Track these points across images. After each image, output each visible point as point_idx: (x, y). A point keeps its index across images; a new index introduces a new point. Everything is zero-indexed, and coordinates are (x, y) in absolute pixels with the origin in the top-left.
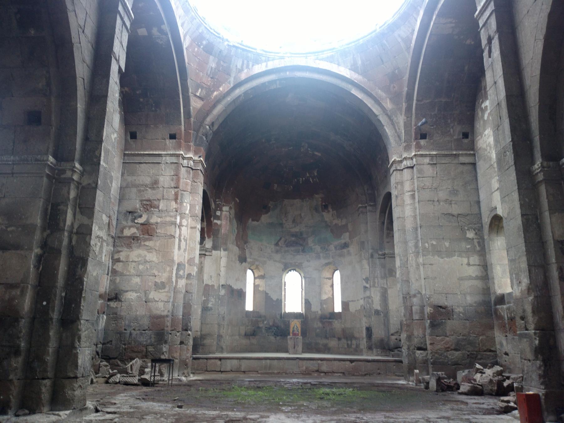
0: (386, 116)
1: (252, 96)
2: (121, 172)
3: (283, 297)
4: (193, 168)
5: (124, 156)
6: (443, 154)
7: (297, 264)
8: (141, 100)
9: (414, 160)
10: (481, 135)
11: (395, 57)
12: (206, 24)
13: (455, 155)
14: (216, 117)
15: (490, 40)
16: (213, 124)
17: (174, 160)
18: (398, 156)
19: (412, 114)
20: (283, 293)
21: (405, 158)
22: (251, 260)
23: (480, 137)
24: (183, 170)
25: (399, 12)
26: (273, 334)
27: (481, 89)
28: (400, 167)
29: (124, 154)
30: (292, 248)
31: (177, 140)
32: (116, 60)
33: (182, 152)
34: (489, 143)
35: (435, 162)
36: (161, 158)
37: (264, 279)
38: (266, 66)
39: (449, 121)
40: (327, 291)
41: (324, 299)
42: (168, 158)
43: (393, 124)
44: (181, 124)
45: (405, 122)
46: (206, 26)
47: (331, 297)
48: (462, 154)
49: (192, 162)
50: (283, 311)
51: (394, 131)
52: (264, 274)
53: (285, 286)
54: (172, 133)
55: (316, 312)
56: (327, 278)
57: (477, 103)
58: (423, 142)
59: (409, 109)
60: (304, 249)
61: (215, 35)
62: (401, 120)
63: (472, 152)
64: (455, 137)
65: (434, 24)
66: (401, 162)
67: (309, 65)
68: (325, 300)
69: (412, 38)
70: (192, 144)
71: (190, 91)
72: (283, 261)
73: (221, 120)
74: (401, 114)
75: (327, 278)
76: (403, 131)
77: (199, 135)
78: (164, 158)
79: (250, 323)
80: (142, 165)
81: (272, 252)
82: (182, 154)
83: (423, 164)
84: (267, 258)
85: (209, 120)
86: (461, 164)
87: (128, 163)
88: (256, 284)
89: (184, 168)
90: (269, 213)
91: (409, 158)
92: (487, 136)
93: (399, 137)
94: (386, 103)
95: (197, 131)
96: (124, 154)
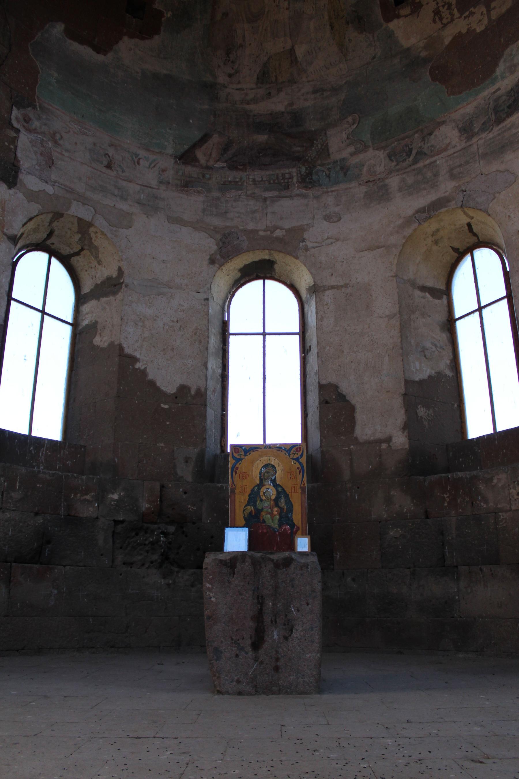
3: (213, 385)
7: (278, 233)
20: (213, 364)
22: (50, 189)
26: (155, 557)
30: (258, 174)
37: (114, 293)
40: (428, 345)
41: (417, 377)
47: (449, 373)
50: (212, 448)
52: (120, 271)
53: (225, 342)
55: (380, 441)
56: (423, 289)
60: (310, 174)
68: (421, 382)
72: (216, 222)
75: (423, 289)
79: (16, 495)
81: (161, 182)
84: (139, 202)
88: (85, 323)
90: (156, 37)
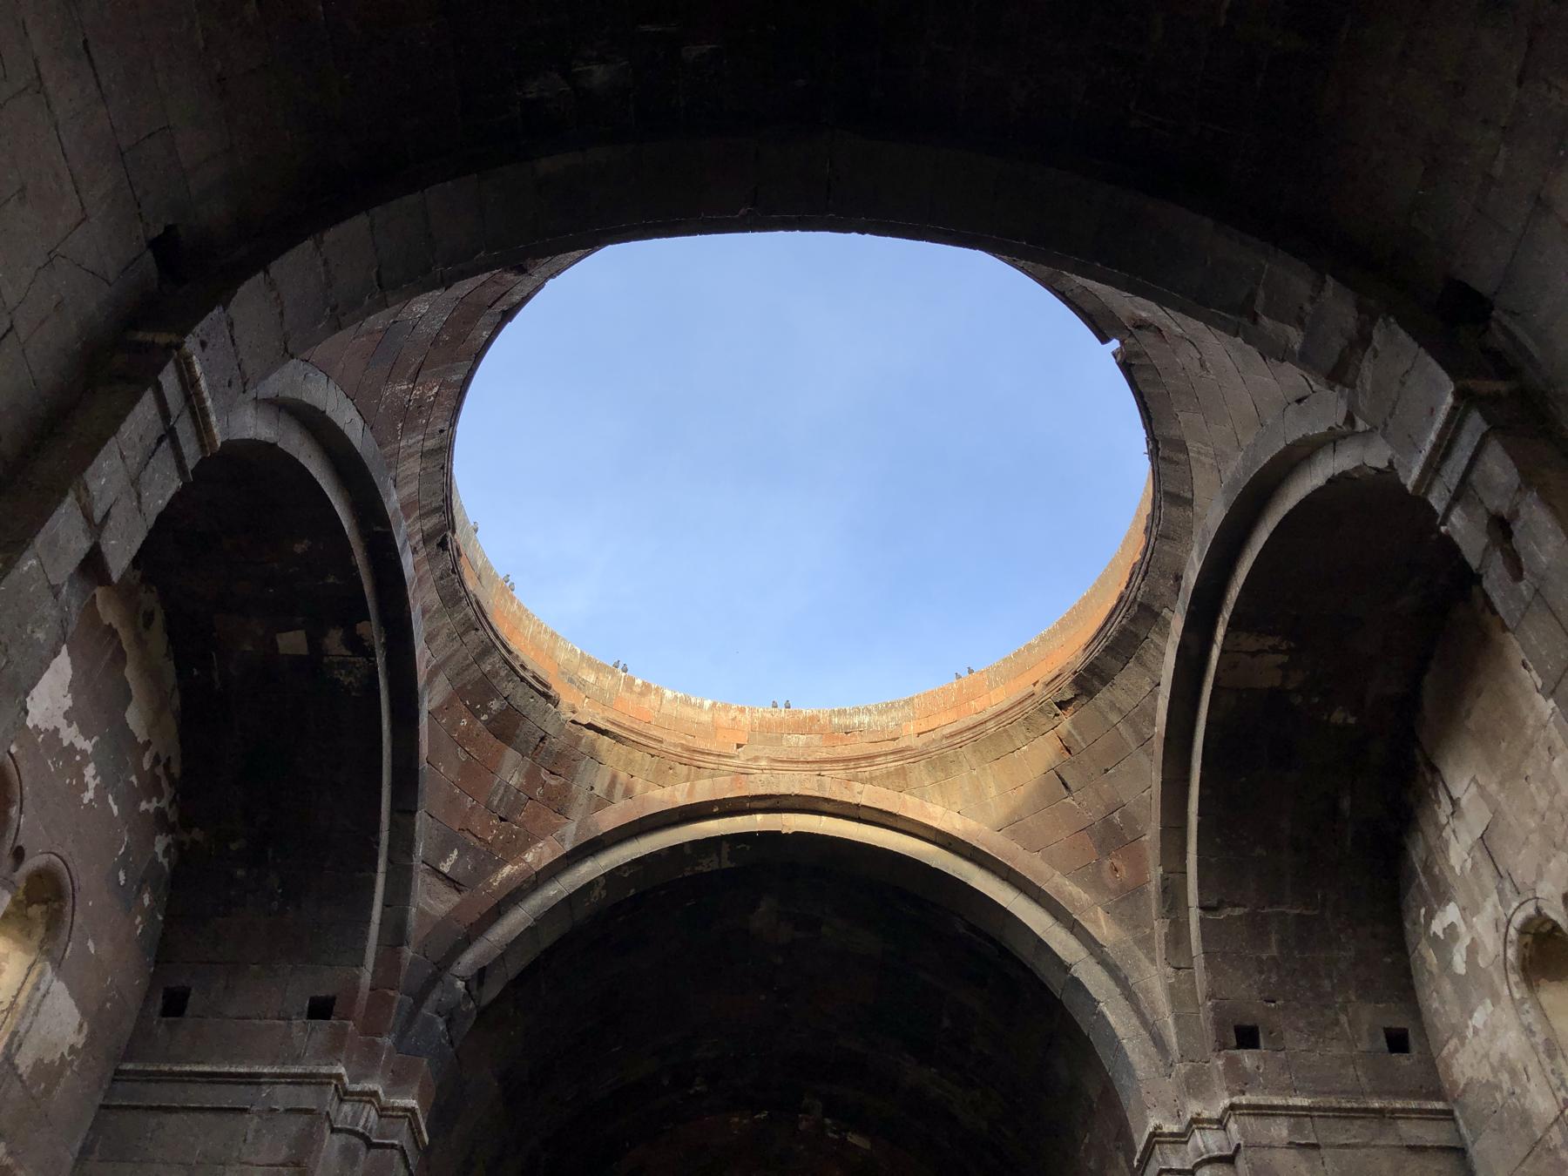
0: (1099, 967)
1: (632, 892)
2: (79, 1144)
4: (375, 1141)
5: (114, 1080)
6: (1334, 1110)
8: (240, 873)
9: (1233, 1126)
10: (1458, 1032)
11: (1107, 770)
12: (509, 652)
13: (1380, 1111)
14: (500, 952)
15: (1501, 527)
16: (481, 975)
17: (306, 1097)
18: (1167, 1114)
19: (1192, 958)
21: (1194, 1121)
23: (1454, 1042)
24: (332, 1144)
25: (1103, 634)
27: (1417, 876)
28: (1183, 1160)
29: (118, 1072)
31: (334, 1021)
32: (88, 517)
33: (342, 1070)
34: (1503, 1056)
35: (1313, 1140)
36: (252, 1089)
38: (691, 792)
39: (1327, 985)
42: (280, 1090)
43: (1129, 995)
44: (360, 963)
45: (1171, 986)
46: (506, 655)
48: (1403, 1110)
49: (373, 1113)
51: (1135, 1021)
54: (321, 993)
57: (1408, 926)
58: (1248, 1058)
59: (1177, 938)
61: (531, 686)
62: (1154, 978)
63: (1439, 1105)
64: (1364, 1045)
65: (1223, 651)
66: (1180, 1138)
67: (827, 796)
69: (1155, 709)
70: (387, 1041)
71: (420, 850)
73: (513, 968)
74: (1153, 961)
76: (1170, 1021)
77: (424, 1011)
78: (265, 1091)
80: (172, 1120)
82: (339, 1077)
83: (1271, 1147)
85: (469, 960)
86: (1412, 1148)
87: (121, 1107)
89: (334, 1137)
91: (1210, 1121)
92: (1483, 1034)
93: (1158, 1041)
94: (1096, 922)
95: (420, 998)
96: (118, 1072)
